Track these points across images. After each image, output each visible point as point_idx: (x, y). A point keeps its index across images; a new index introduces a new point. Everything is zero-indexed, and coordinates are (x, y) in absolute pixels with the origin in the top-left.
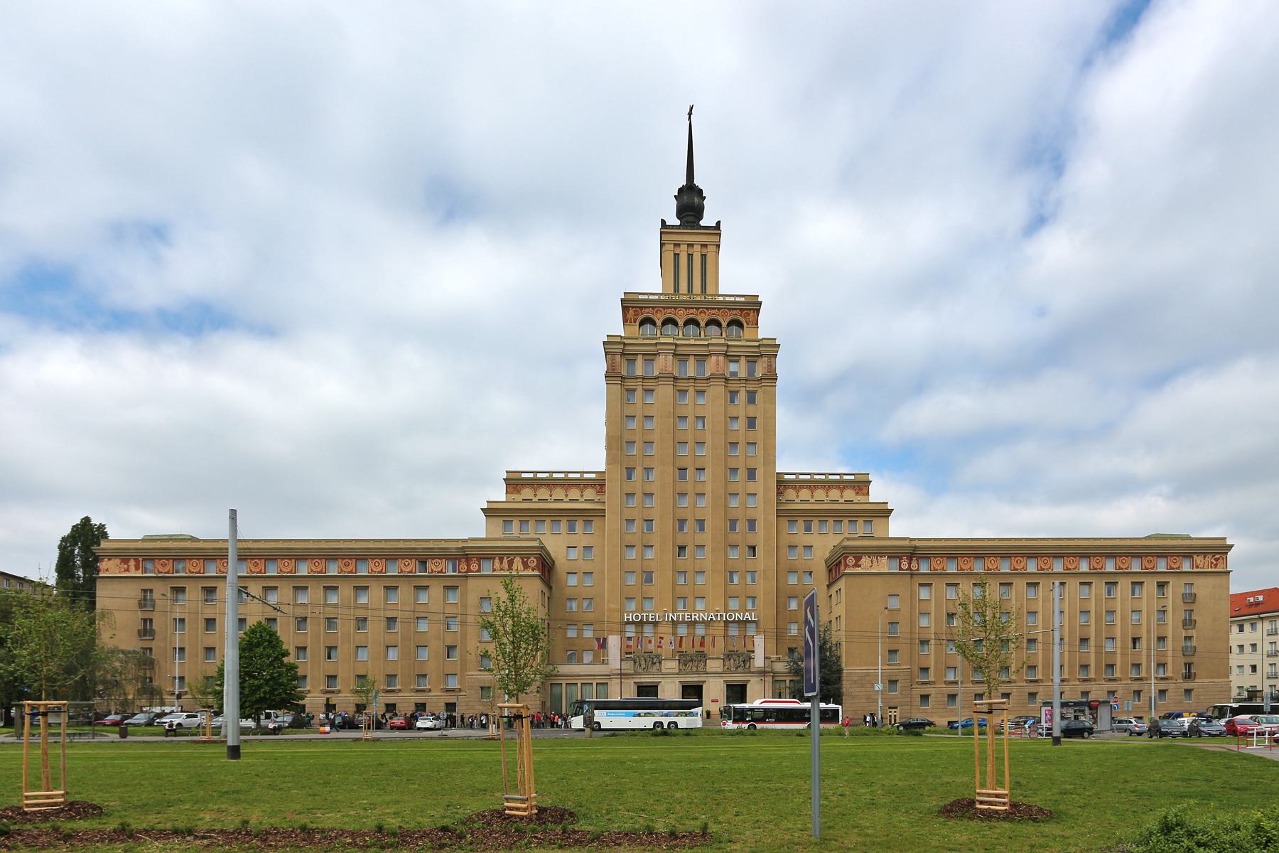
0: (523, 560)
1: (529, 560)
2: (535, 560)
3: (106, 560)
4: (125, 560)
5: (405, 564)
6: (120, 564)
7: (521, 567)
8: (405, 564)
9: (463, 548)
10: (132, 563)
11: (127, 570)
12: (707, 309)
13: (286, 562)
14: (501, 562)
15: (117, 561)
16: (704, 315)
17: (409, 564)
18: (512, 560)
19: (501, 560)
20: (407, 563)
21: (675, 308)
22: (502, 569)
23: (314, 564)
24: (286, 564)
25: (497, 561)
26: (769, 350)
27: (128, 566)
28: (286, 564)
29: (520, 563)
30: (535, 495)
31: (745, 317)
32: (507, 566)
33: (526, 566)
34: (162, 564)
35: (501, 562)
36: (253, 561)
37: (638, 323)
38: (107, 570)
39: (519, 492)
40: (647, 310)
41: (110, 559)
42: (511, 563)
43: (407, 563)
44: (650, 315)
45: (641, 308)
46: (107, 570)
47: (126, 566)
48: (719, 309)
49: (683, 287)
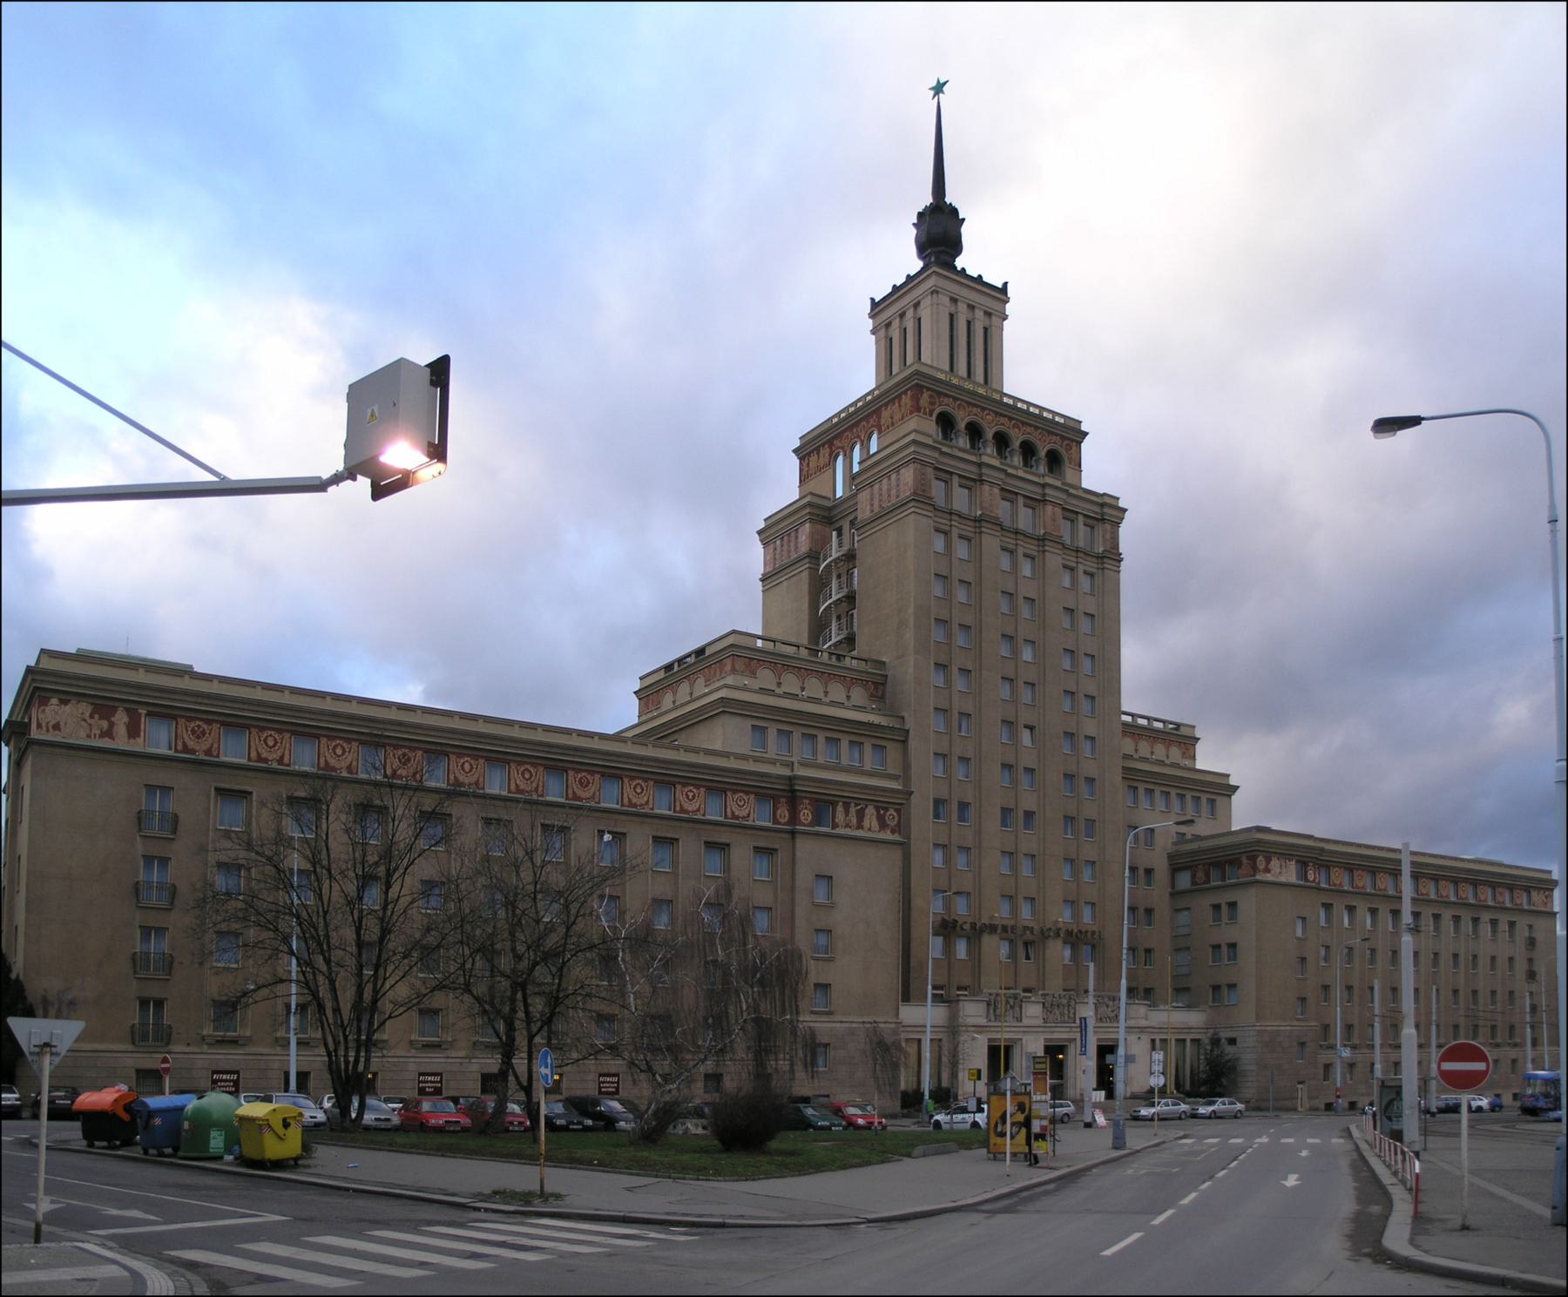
0: (878, 812)
1: (888, 814)
2: (895, 814)
3: (54, 701)
4: (103, 708)
5: (687, 796)
6: (91, 716)
7: (875, 824)
8: (687, 796)
9: (790, 778)
10: (121, 718)
11: (108, 734)
12: (1024, 423)
13: (467, 762)
14: (847, 815)
15: (85, 708)
16: (1016, 430)
17: (694, 796)
18: (863, 810)
19: (847, 806)
20: (691, 794)
21: (983, 409)
22: (847, 826)
23: (523, 774)
24: (467, 766)
25: (840, 809)
26: (1106, 512)
27: (112, 725)
28: (467, 766)
29: (874, 818)
30: (779, 684)
31: (1066, 450)
32: (854, 820)
33: (883, 825)
34: (193, 731)
35: (847, 815)
36: (400, 752)
37: (934, 418)
38: (57, 727)
39: (753, 674)
40: (946, 400)
41: (64, 702)
42: (861, 815)
43: (691, 794)
44: (949, 409)
45: (939, 394)
46: (57, 727)
47: (105, 724)
48: (1037, 428)
49: (962, 369)
